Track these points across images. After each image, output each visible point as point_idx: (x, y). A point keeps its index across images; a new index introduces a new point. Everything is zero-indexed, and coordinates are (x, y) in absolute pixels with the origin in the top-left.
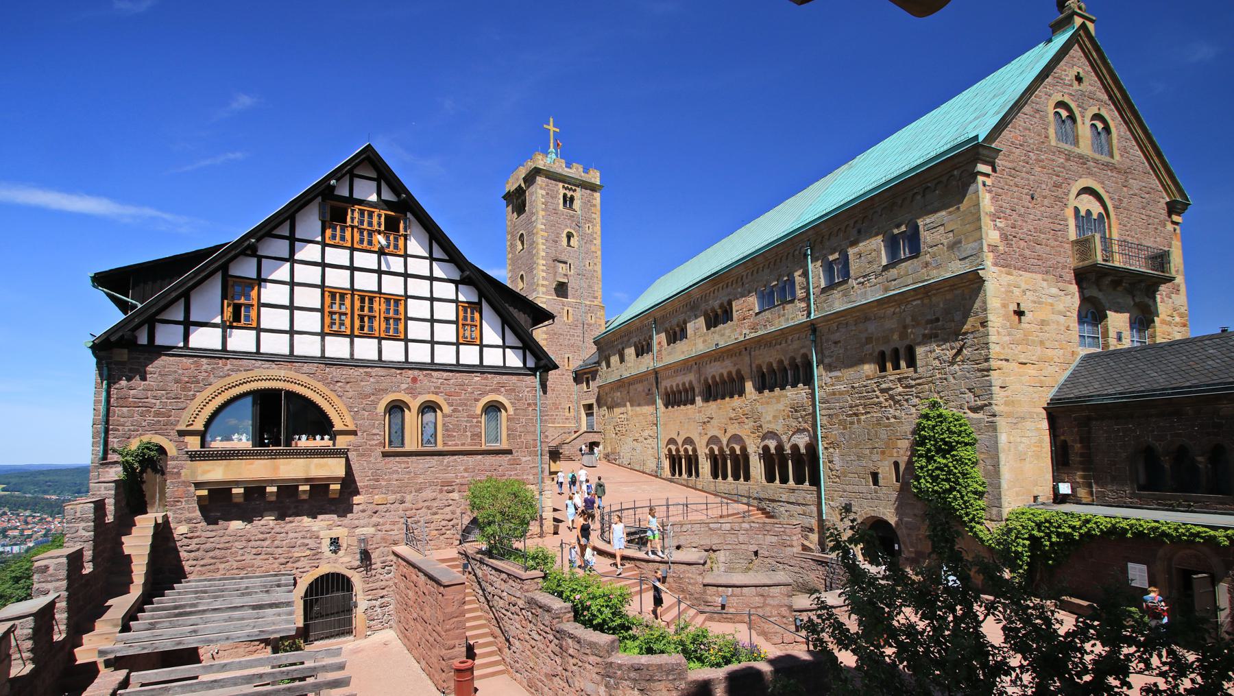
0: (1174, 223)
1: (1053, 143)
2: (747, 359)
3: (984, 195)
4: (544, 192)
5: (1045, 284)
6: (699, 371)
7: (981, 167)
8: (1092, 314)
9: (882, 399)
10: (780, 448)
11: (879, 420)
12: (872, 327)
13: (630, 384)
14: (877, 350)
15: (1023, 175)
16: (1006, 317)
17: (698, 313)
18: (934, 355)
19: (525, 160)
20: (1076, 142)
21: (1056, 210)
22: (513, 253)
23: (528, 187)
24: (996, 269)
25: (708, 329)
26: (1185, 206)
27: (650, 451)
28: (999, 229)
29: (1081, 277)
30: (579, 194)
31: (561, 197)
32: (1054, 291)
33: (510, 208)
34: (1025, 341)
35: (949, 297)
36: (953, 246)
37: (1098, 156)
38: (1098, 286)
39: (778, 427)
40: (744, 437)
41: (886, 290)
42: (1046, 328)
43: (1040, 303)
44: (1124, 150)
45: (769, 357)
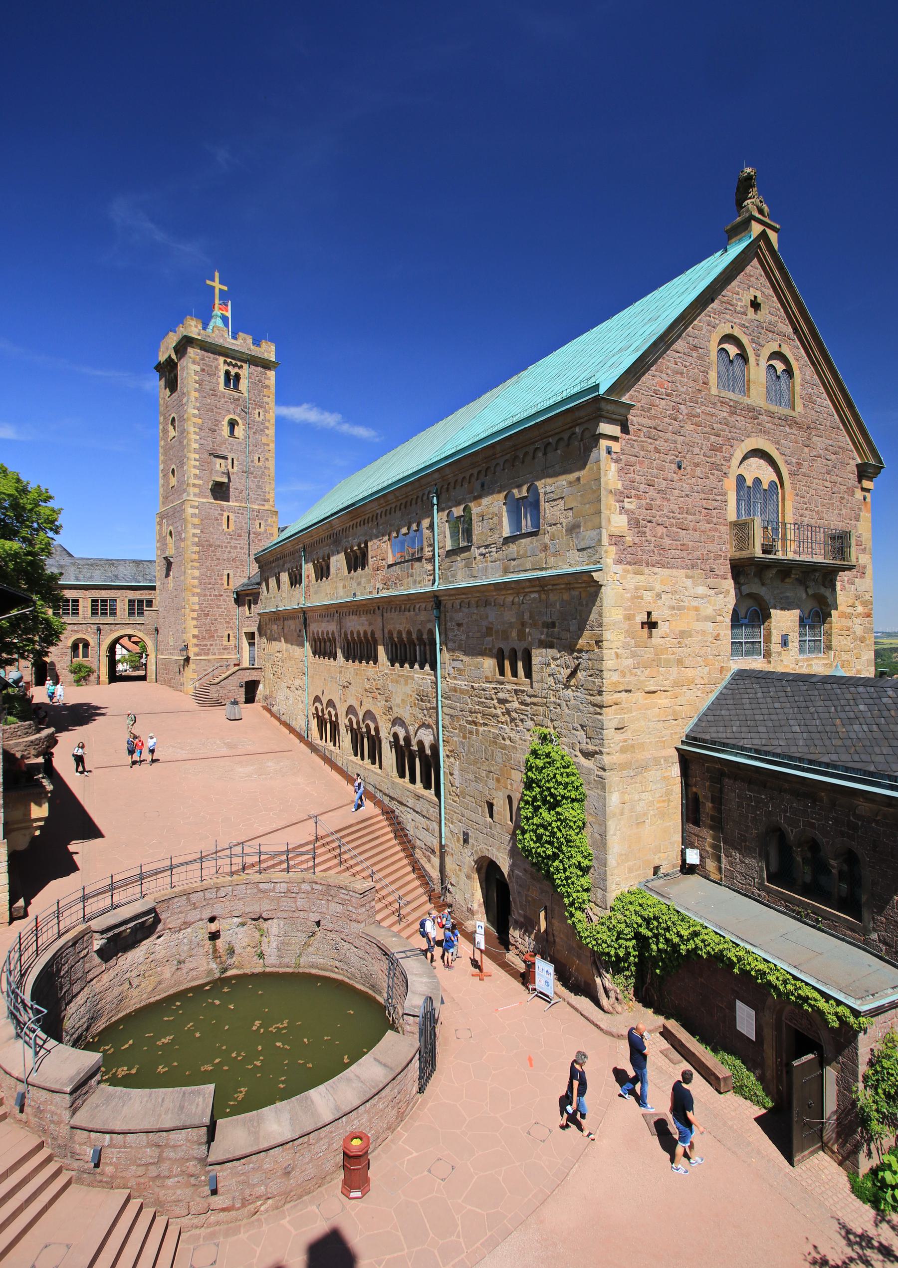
0: (863, 489)
1: (714, 391)
2: (380, 620)
3: (608, 467)
4: (198, 368)
5: (689, 582)
6: (340, 622)
7: (605, 428)
8: (750, 615)
9: (499, 712)
10: (407, 739)
11: (496, 736)
12: (492, 615)
13: (285, 619)
14: (497, 647)
15: (669, 435)
16: (630, 633)
17: (340, 549)
18: (548, 670)
19: (177, 325)
20: (745, 389)
21: (712, 481)
22: (166, 441)
23: (179, 359)
24: (619, 568)
25: (349, 573)
26: (878, 469)
27: (300, 706)
28: (627, 512)
29: (742, 570)
30: (245, 371)
31: (222, 375)
32: (701, 590)
33: (162, 383)
34: (657, 662)
35: (566, 597)
36: (573, 529)
37: (773, 408)
38: (761, 579)
39: (405, 713)
40: (377, 717)
41: (506, 571)
42: (687, 641)
43: (679, 608)
44: (809, 400)
45: (400, 624)
